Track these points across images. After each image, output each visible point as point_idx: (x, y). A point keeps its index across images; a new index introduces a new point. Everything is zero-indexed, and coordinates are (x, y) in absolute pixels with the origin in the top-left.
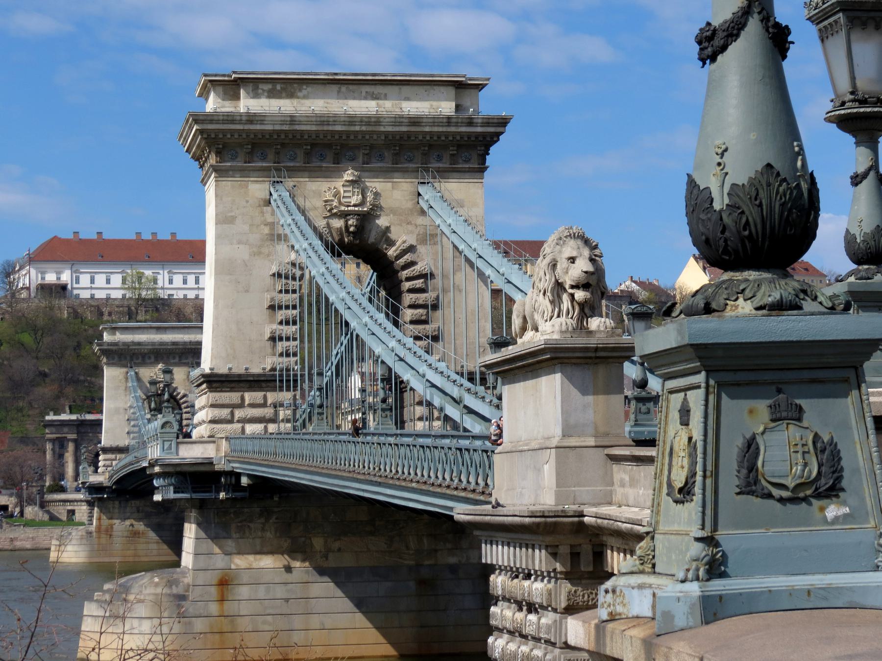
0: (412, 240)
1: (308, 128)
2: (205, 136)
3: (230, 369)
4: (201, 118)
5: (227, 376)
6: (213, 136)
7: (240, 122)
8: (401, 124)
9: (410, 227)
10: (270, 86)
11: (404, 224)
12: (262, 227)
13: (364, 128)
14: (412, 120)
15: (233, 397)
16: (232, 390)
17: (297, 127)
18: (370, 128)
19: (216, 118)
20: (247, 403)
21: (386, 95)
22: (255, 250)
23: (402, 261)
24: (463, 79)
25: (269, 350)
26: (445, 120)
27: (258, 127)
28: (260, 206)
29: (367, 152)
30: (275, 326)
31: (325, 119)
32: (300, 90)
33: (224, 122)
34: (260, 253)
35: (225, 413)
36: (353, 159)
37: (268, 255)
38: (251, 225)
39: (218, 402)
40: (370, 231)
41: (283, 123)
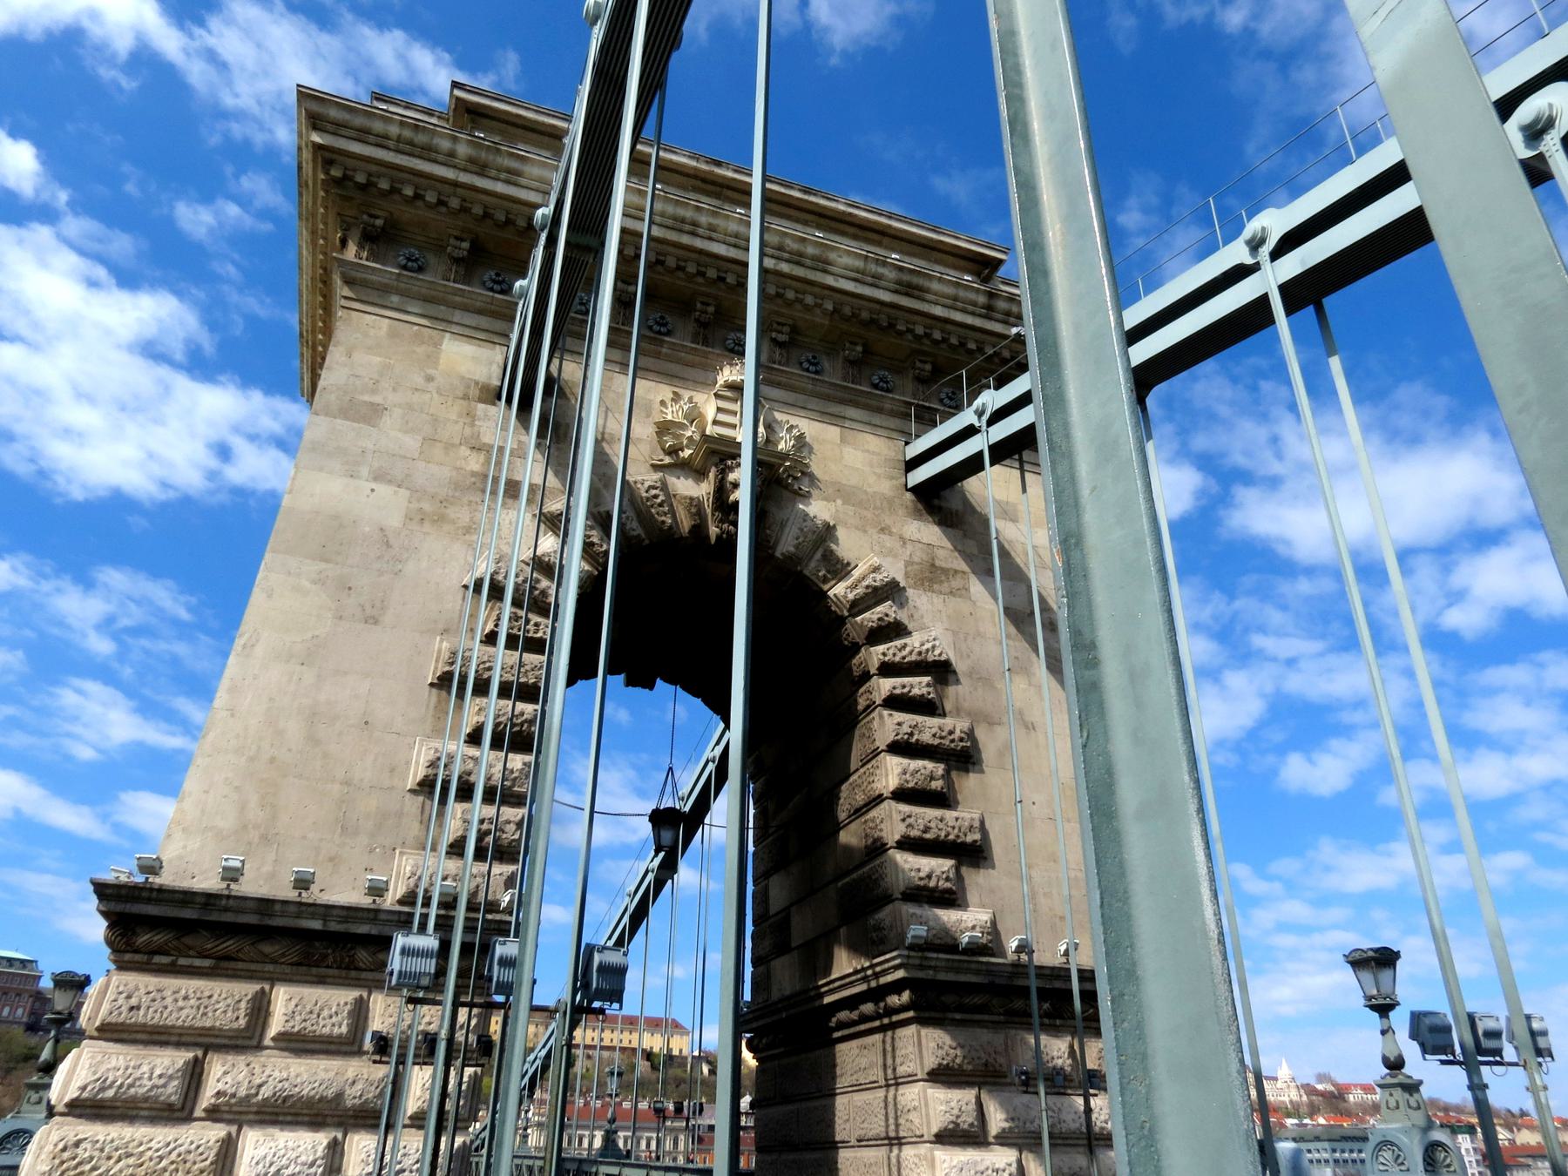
0: (894, 570)
2: (336, 172)
3: (232, 875)
4: (333, 113)
5: (209, 900)
6: (361, 178)
9: (888, 541)
11: (872, 531)
12: (464, 451)
13: (785, 267)
14: (906, 277)
15: (219, 1000)
16: (223, 967)
18: (800, 272)
20: (276, 1026)
22: (427, 506)
23: (870, 617)
25: (415, 829)
27: (500, 187)
28: (466, 397)
30: (457, 747)
34: (440, 519)
35: (158, 1068)
37: (468, 530)
38: (430, 440)
39: (139, 1018)
40: (783, 525)
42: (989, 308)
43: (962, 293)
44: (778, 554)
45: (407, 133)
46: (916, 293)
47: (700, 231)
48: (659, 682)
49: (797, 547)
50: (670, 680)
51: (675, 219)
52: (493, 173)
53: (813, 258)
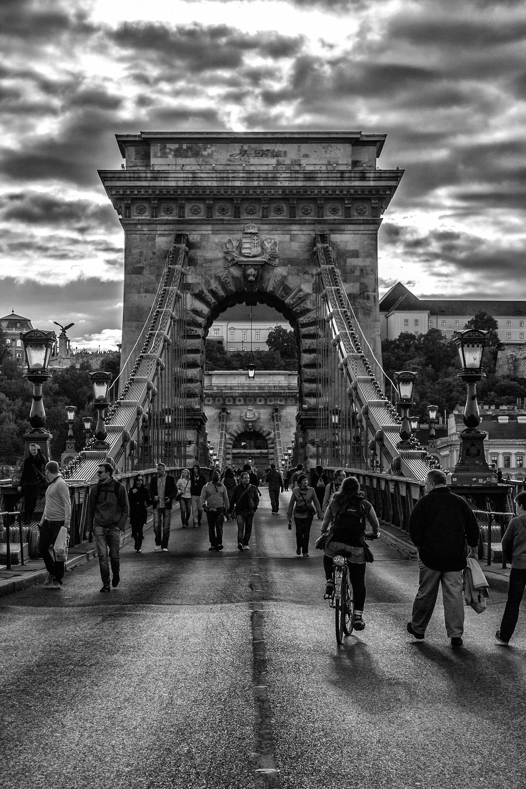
1: (209, 184)
4: (109, 175)
7: (146, 179)
8: (296, 179)
9: (307, 277)
10: (177, 146)
13: (262, 184)
14: (308, 175)
17: (199, 184)
19: (123, 175)
21: (285, 152)
24: (359, 136)
26: (339, 175)
27: (163, 184)
29: (266, 206)
31: (225, 175)
32: (205, 149)
33: (130, 179)
36: (251, 212)
40: (269, 280)
41: (186, 179)
42: (342, 177)
43: (330, 175)
45: (132, 175)
46: (312, 179)
47: (230, 179)
48: (258, 303)
49: (273, 288)
50: (262, 303)
52: (160, 179)
53: (271, 178)
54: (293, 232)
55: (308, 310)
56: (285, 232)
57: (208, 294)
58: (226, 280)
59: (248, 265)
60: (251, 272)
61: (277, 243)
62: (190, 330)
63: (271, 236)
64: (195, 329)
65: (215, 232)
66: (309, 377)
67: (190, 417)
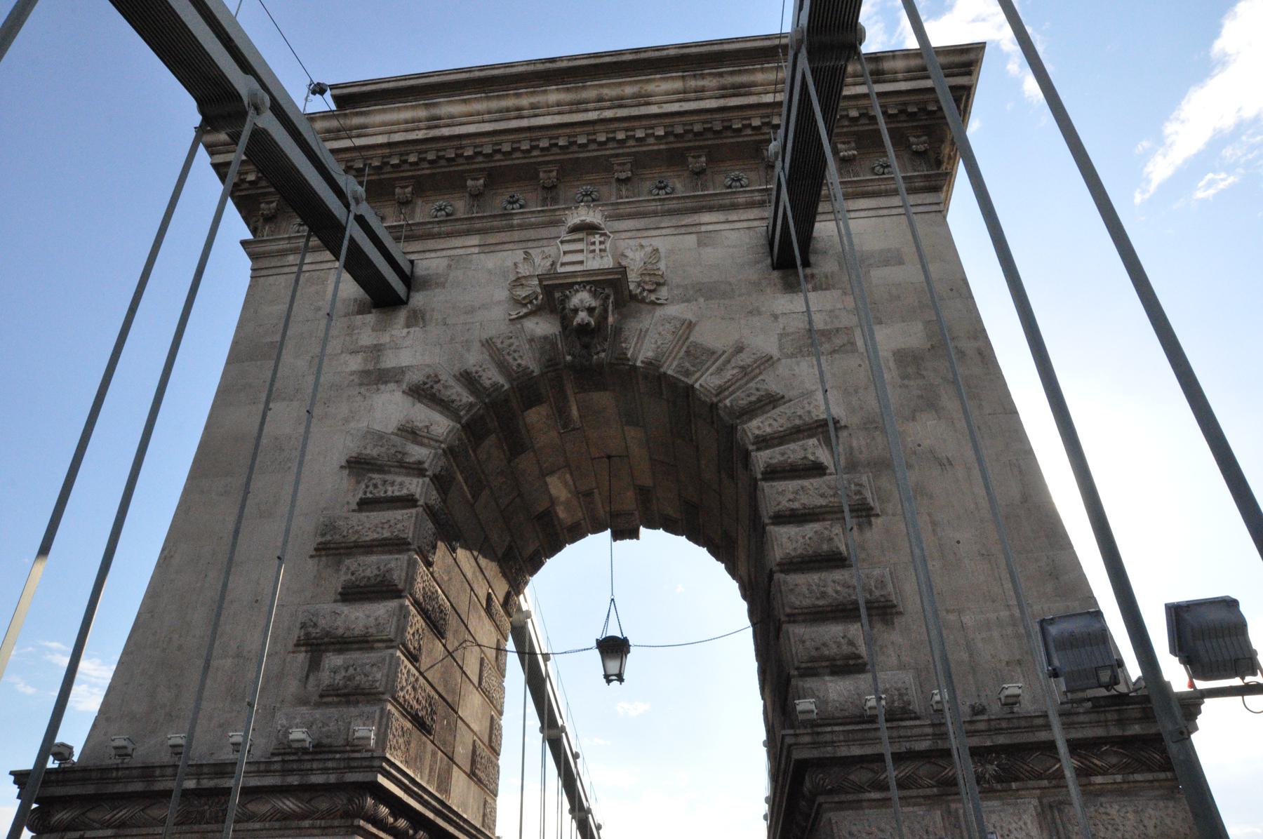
29: (623, 176)
44: (639, 364)
46: (743, 90)
47: (525, 112)
48: (643, 531)
50: (651, 525)
51: (500, 111)
53: (635, 96)
54: (703, 228)
55: (772, 401)
56: (683, 230)
57: (452, 382)
58: (510, 345)
59: (571, 285)
60: (582, 301)
61: (662, 250)
62: (385, 482)
63: (644, 242)
64: (399, 479)
65: (485, 248)
66: (807, 602)
67: (332, 779)
